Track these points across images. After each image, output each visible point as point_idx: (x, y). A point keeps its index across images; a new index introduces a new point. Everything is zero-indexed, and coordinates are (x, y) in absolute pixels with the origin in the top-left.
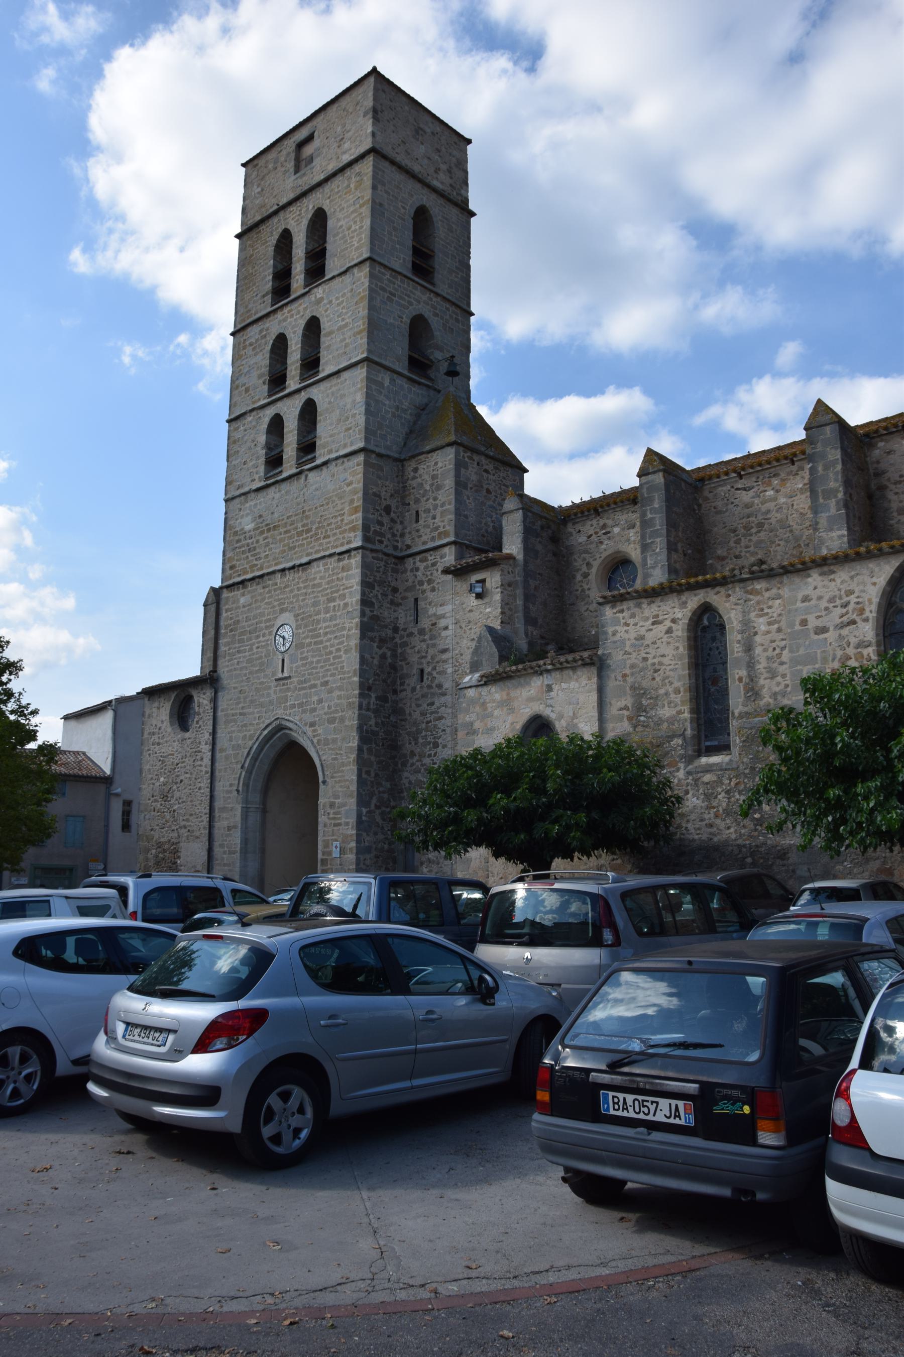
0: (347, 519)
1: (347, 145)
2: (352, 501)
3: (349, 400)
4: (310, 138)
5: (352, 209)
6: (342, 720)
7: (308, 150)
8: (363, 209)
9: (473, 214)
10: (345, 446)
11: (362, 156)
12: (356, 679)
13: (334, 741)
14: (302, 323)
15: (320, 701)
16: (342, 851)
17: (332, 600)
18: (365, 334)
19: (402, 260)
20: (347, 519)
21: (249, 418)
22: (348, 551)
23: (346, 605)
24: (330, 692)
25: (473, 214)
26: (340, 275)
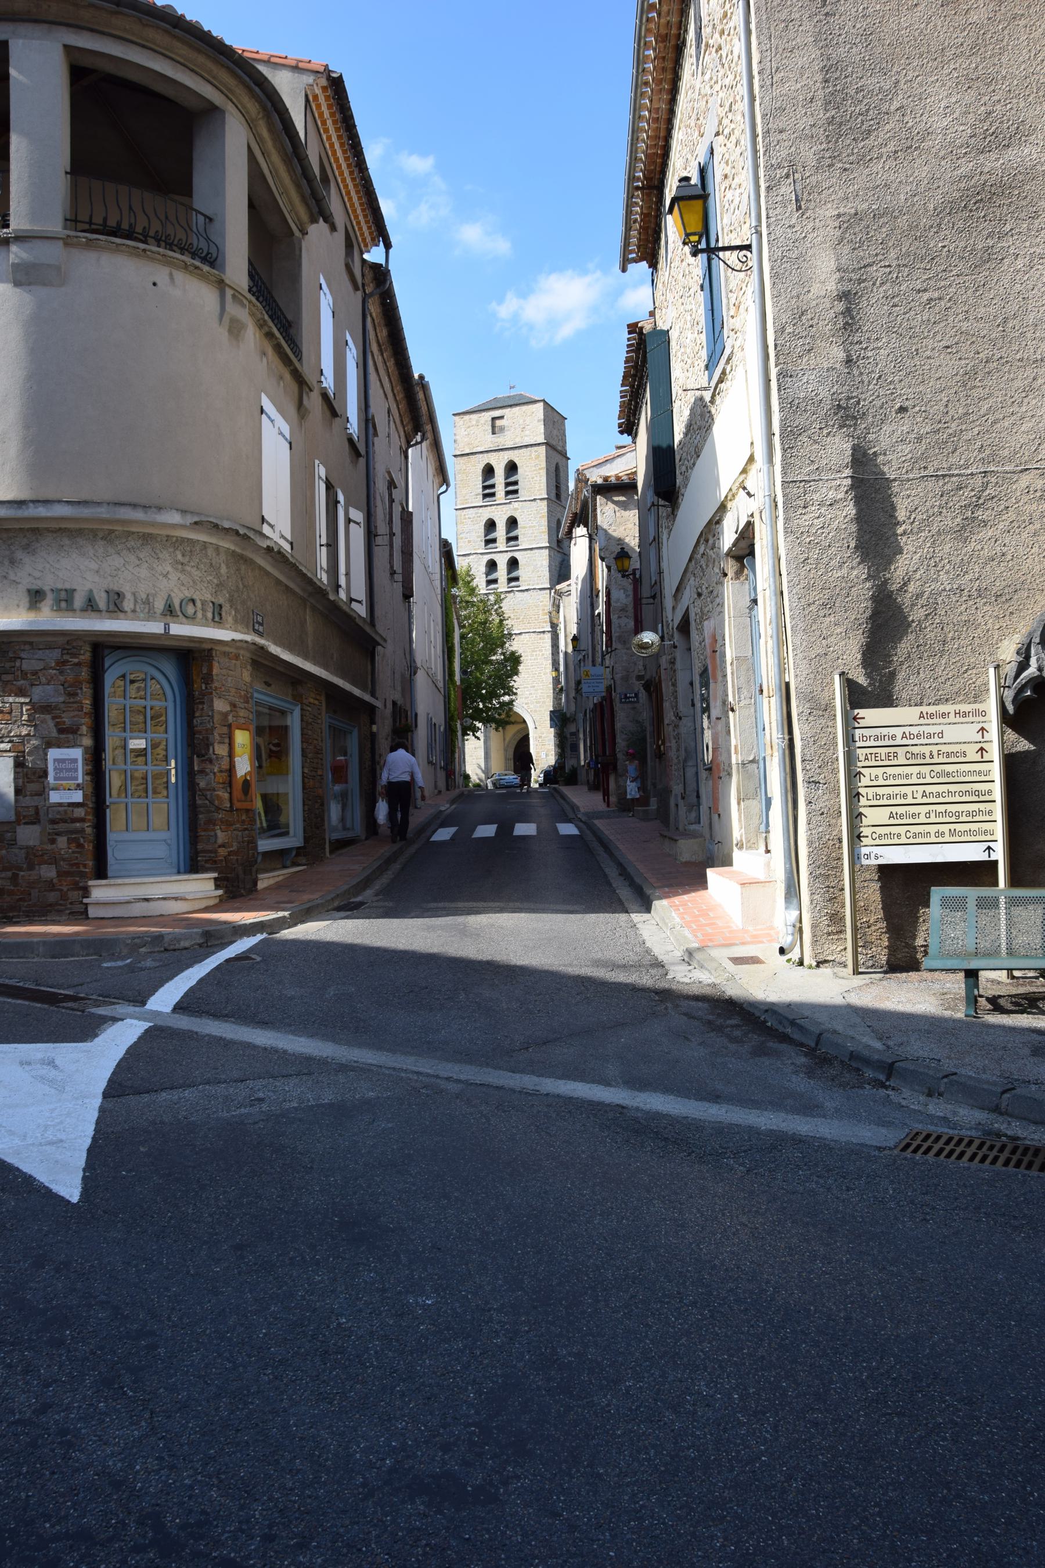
0: (541, 617)
1: (527, 432)
2: (544, 610)
3: (539, 564)
4: (502, 417)
5: (534, 468)
6: (544, 702)
7: (498, 423)
8: (541, 471)
9: (569, 459)
10: (538, 584)
11: (539, 444)
12: (551, 686)
13: (540, 711)
14: (506, 517)
15: (531, 694)
16: (547, 755)
17: (533, 651)
18: (547, 534)
19: (553, 496)
20: (541, 617)
21: (471, 557)
22: (544, 632)
23: (543, 655)
24: (536, 690)
25: (569, 459)
26: (532, 500)
